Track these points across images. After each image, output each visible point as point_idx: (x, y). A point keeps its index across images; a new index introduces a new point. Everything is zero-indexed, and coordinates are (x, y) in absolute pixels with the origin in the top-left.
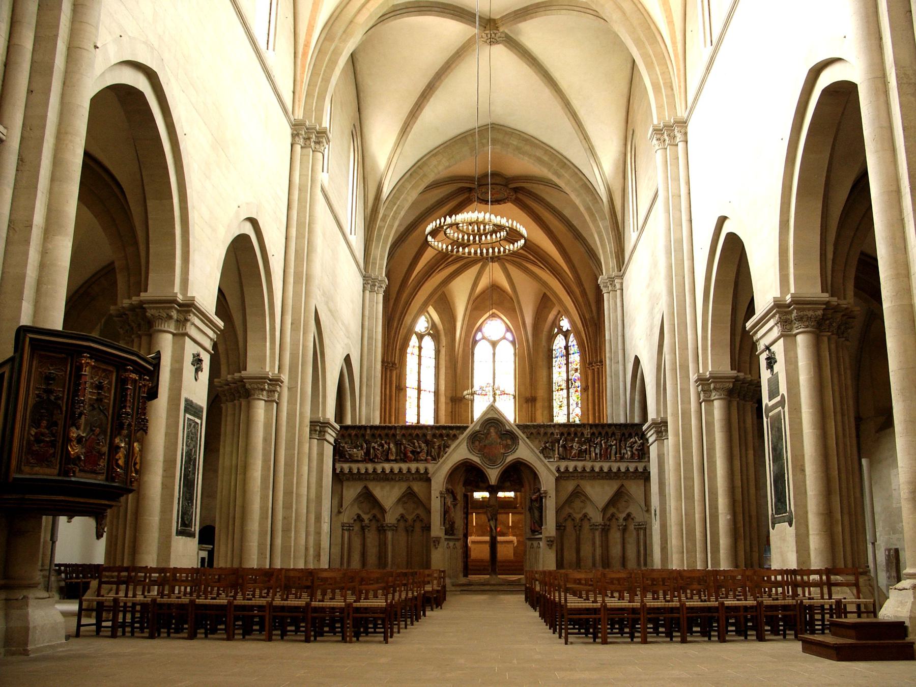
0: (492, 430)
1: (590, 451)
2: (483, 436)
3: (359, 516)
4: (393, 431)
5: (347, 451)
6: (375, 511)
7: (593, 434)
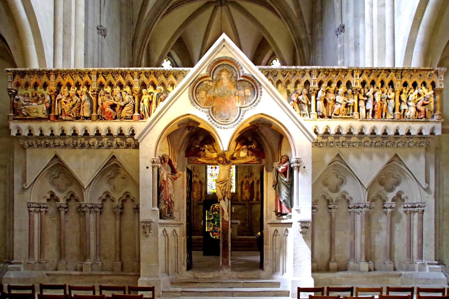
0: (224, 75)
1: (359, 108)
2: (211, 84)
3: (52, 195)
4: (86, 78)
5: (23, 105)
6: (70, 189)
7: (363, 84)
